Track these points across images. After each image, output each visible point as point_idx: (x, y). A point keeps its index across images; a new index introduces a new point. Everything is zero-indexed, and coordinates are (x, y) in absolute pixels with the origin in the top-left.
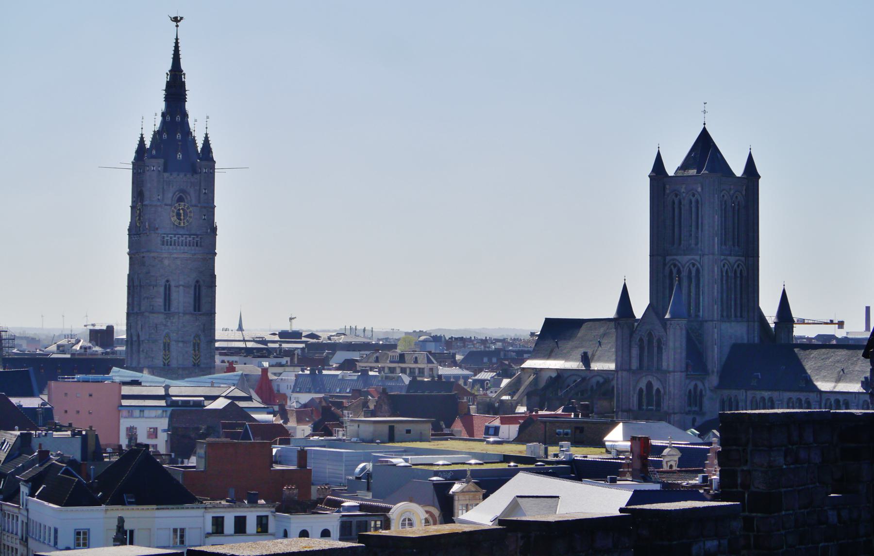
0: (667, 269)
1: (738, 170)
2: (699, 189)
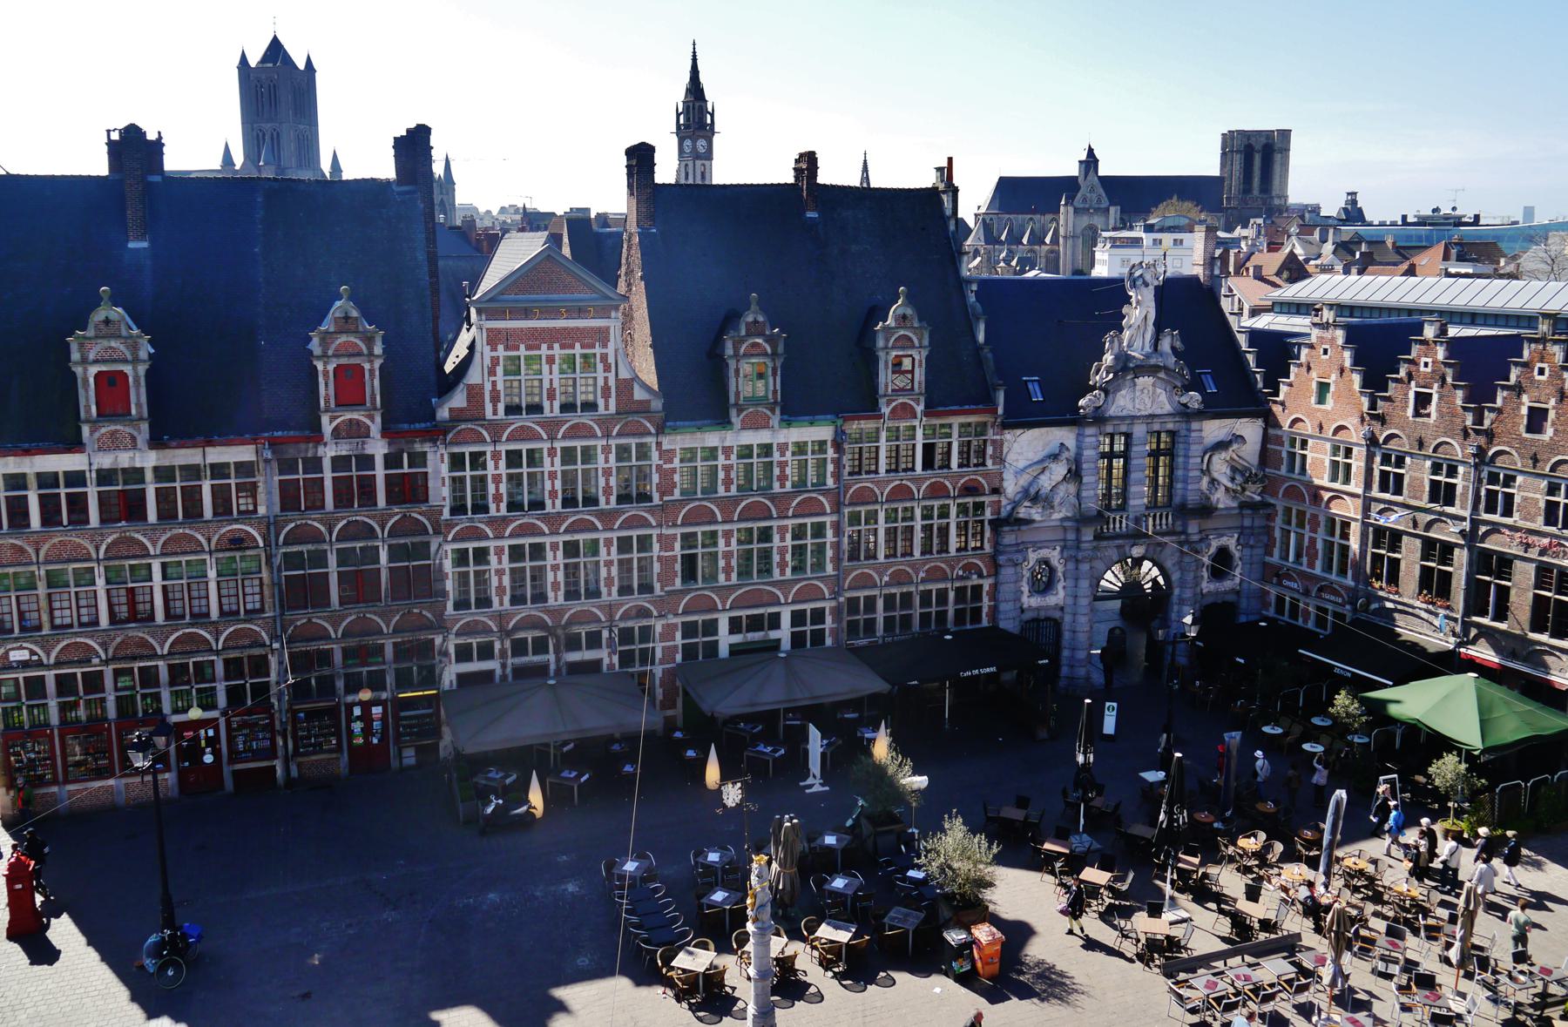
0: (255, 134)
1: (301, 65)
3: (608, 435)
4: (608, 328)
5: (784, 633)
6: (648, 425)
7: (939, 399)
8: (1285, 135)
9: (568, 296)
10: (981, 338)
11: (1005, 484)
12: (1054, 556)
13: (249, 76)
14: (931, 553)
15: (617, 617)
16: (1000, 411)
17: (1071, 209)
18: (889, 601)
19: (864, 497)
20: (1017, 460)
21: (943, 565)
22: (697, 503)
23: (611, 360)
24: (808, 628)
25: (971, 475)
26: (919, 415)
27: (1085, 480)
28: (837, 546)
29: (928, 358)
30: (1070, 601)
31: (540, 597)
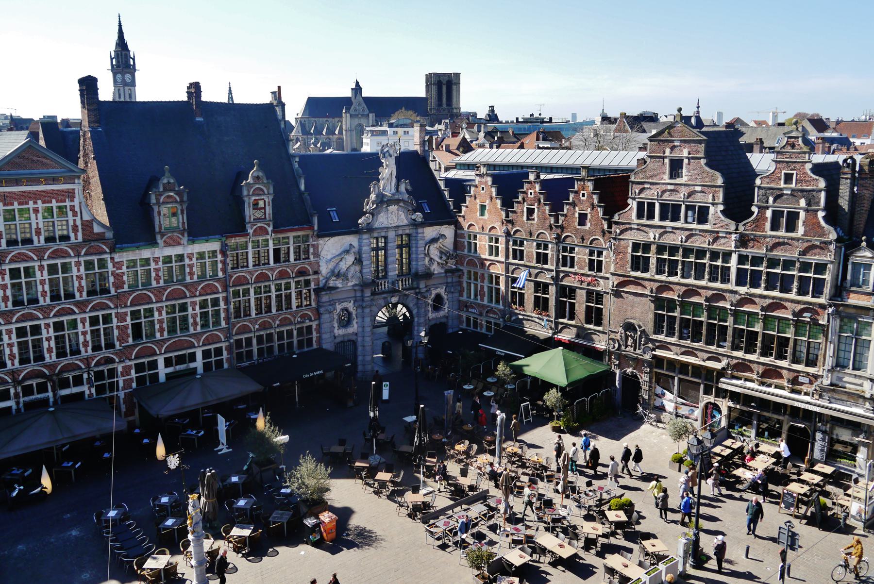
3: (78, 255)
4: (73, 190)
5: (199, 364)
6: (104, 247)
7: (281, 223)
8: (457, 75)
9: (45, 171)
10: (303, 187)
11: (321, 268)
12: (350, 306)
14: (282, 310)
15: (92, 365)
16: (316, 228)
17: (348, 115)
18: (260, 339)
19: (241, 281)
20: (327, 255)
21: (289, 316)
22: (139, 292)
23: (77, 209)
24: (213, 359)
25: (301, 265)
26: (270, 233)
27: (364, 263)
28: (227, 311)
29: (273, 200)
30: (360, 330)
31: (40, 357)
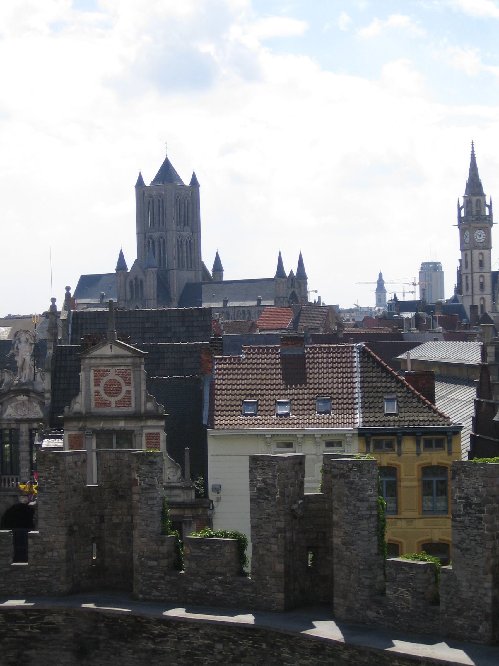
1: (187, 181)
2: (163, 193)
13: (144, 193)
